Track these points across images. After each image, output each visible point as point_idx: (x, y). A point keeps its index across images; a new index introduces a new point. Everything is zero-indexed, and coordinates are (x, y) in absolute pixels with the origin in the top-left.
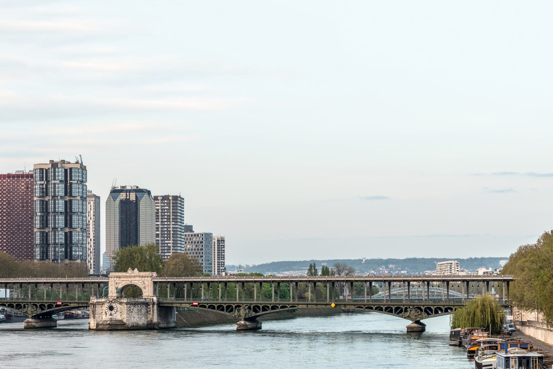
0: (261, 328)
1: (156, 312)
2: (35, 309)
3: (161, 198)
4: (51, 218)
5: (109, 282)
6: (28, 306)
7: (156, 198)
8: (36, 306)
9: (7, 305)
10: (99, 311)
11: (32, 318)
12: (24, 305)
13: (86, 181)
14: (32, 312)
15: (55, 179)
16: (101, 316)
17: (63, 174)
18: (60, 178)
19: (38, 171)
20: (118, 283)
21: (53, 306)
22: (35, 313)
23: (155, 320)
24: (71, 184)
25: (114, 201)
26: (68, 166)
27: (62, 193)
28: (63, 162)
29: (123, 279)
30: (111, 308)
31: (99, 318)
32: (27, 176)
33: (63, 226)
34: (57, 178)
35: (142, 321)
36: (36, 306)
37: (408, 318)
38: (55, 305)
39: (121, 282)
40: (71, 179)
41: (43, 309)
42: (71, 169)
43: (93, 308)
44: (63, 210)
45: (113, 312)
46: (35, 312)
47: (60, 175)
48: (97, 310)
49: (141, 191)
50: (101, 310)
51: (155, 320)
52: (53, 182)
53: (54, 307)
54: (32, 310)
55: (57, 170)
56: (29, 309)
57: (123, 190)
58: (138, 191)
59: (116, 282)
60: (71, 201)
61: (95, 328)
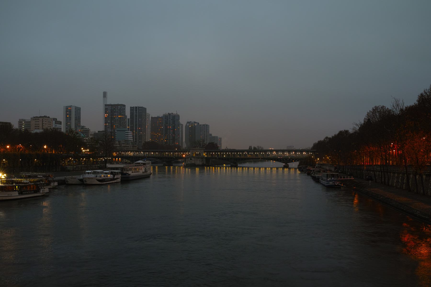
0: (238, 166)
1: (205, 160)
11: (166, 162)
13: (179, 120)
15: (170, 119)
18: (171, 118)
23: (205, 163)
24: (175, 120)
26: (173, 115)
28: (172, 113)
29: (194, 150)
30: (191, 159)
32: (161, 118)
35: (201, 163)
37: (284, 163)
42: (175, 116)
45: (191, 160)
49: (196, 123)
51: (205, 163)
58: (195, 123)
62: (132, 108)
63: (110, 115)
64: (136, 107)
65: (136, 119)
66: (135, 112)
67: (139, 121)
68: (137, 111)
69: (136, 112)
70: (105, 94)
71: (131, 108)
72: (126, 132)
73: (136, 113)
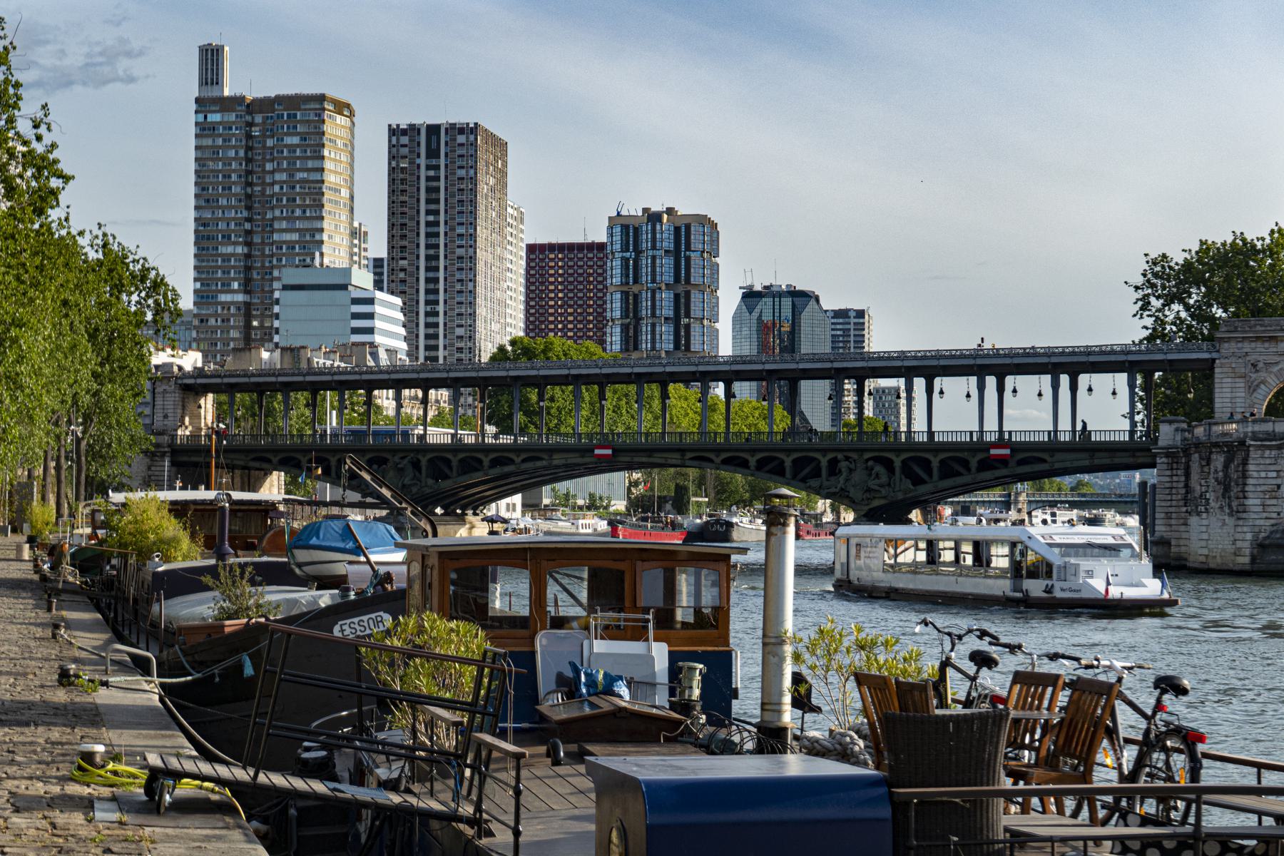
2: (884, 479)
3: (832, 314)
4: (645, 328)
5: (1214, 360)
6: (852, 466)
7: (826, 311)
8: (888, 465)
9: (753, 461)
10: (1261, 481)
12: (833, 463)
14: (869, 490)
16: (1274, 502)
17: (672, 237)
19: (619, 229)
20: (1261, 365)
21: (965, 463)
22: (885, 497)
24: (688, 259)
25: (750, 313)
27: (668, 277)
28: (670, 211)
31: (1265, 515)
33: (672, 346)
34: (658, 244)
36: (888, 465)
38: (980, 462)
39: (1277, 359)
40: (688, 248)
41: (917, 481)
43: (1226, 467)
44: (671, 314)
46: (884, 492)
47: (666, 240)
48: (1255, 474)
50: (1274, 474)
52: (650, 253)
53: (973, 470)
54: (872, 484)
55: (658, 227)
56: (858, 476)
57: (769, 292)
59: (1252, 358)
60: (688, 294)
61: (1246, 560)
62: (404, 132)
63: (234, 177)
64: (433, 130)
65: (431, 275)
66: (428, 168)
67: (453, 229)
68: (438, 157)
69: (434, 162)
70: (211, 59)
71: (394, 132)
72: (356, 301)
73: (432, 173)
